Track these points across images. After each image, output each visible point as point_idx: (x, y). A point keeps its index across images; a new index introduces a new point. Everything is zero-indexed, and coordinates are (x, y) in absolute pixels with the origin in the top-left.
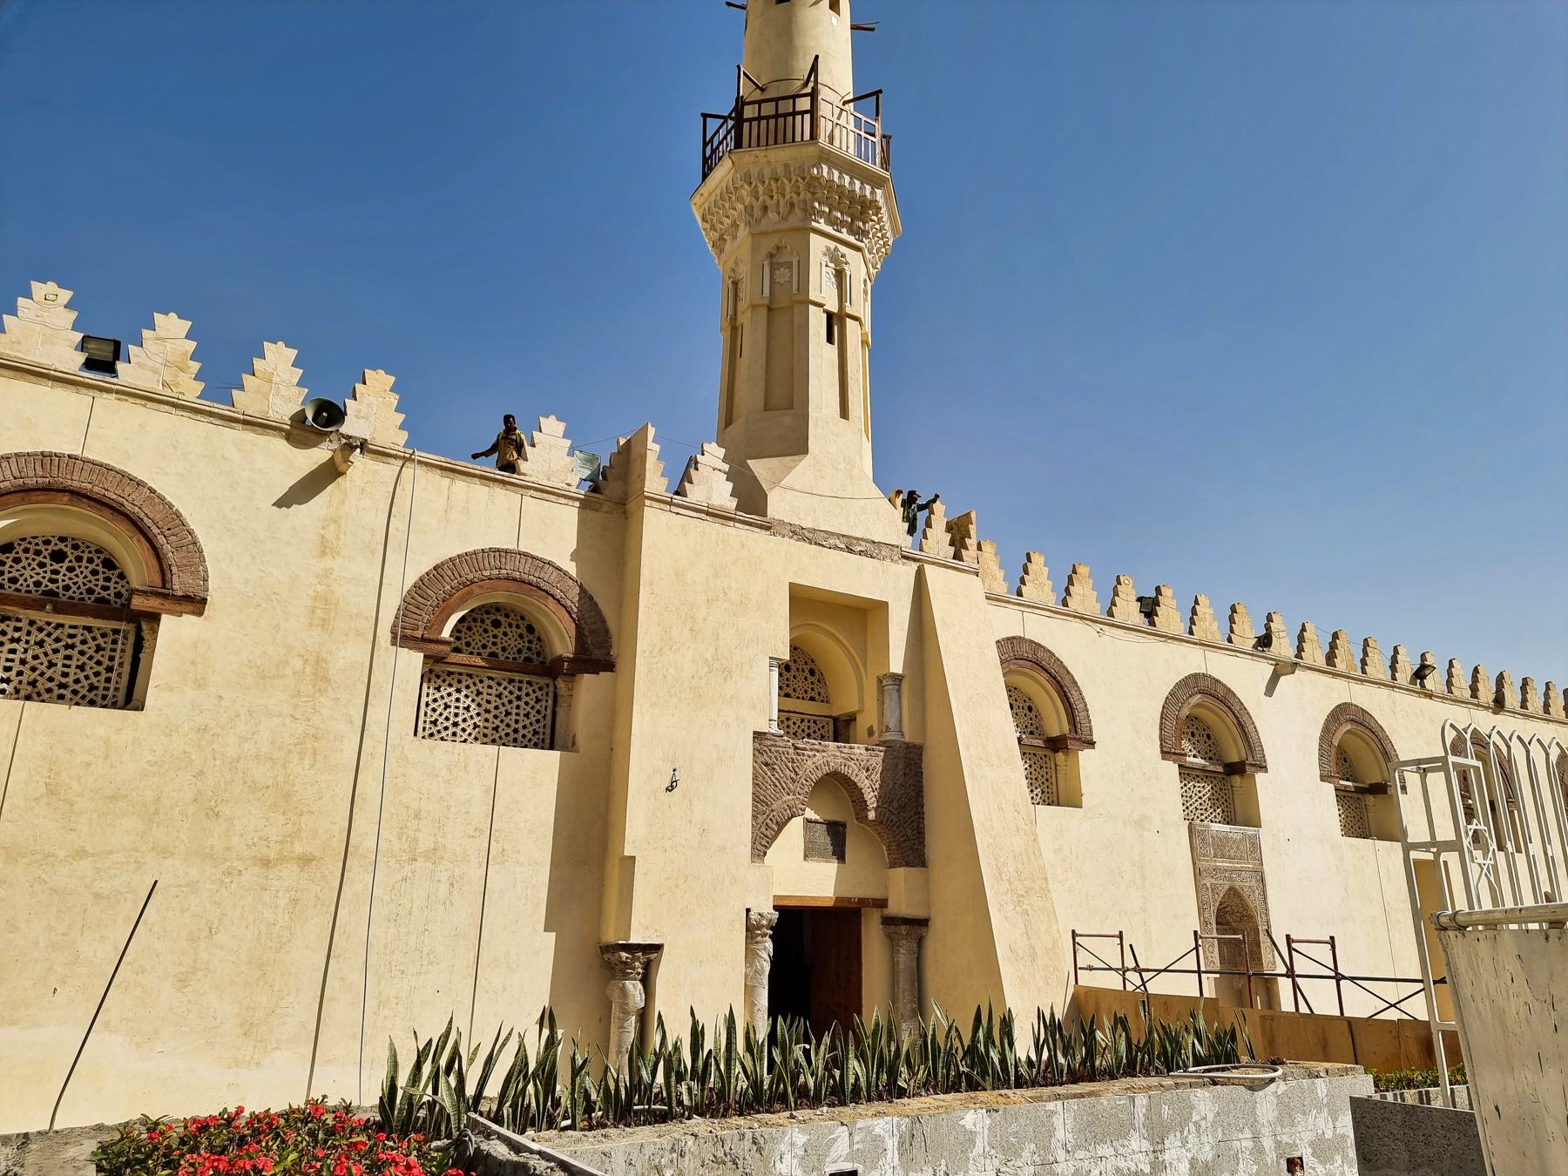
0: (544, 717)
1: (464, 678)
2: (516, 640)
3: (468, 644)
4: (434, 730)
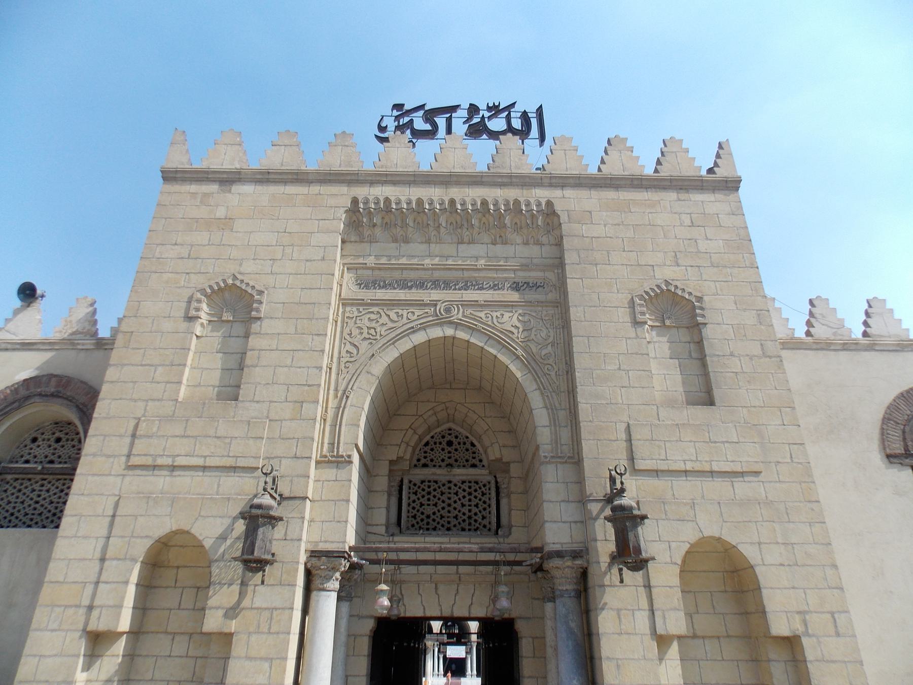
0: (489, 506)
2: (464, 453)
3: (432, 460)
4: (414, 522)
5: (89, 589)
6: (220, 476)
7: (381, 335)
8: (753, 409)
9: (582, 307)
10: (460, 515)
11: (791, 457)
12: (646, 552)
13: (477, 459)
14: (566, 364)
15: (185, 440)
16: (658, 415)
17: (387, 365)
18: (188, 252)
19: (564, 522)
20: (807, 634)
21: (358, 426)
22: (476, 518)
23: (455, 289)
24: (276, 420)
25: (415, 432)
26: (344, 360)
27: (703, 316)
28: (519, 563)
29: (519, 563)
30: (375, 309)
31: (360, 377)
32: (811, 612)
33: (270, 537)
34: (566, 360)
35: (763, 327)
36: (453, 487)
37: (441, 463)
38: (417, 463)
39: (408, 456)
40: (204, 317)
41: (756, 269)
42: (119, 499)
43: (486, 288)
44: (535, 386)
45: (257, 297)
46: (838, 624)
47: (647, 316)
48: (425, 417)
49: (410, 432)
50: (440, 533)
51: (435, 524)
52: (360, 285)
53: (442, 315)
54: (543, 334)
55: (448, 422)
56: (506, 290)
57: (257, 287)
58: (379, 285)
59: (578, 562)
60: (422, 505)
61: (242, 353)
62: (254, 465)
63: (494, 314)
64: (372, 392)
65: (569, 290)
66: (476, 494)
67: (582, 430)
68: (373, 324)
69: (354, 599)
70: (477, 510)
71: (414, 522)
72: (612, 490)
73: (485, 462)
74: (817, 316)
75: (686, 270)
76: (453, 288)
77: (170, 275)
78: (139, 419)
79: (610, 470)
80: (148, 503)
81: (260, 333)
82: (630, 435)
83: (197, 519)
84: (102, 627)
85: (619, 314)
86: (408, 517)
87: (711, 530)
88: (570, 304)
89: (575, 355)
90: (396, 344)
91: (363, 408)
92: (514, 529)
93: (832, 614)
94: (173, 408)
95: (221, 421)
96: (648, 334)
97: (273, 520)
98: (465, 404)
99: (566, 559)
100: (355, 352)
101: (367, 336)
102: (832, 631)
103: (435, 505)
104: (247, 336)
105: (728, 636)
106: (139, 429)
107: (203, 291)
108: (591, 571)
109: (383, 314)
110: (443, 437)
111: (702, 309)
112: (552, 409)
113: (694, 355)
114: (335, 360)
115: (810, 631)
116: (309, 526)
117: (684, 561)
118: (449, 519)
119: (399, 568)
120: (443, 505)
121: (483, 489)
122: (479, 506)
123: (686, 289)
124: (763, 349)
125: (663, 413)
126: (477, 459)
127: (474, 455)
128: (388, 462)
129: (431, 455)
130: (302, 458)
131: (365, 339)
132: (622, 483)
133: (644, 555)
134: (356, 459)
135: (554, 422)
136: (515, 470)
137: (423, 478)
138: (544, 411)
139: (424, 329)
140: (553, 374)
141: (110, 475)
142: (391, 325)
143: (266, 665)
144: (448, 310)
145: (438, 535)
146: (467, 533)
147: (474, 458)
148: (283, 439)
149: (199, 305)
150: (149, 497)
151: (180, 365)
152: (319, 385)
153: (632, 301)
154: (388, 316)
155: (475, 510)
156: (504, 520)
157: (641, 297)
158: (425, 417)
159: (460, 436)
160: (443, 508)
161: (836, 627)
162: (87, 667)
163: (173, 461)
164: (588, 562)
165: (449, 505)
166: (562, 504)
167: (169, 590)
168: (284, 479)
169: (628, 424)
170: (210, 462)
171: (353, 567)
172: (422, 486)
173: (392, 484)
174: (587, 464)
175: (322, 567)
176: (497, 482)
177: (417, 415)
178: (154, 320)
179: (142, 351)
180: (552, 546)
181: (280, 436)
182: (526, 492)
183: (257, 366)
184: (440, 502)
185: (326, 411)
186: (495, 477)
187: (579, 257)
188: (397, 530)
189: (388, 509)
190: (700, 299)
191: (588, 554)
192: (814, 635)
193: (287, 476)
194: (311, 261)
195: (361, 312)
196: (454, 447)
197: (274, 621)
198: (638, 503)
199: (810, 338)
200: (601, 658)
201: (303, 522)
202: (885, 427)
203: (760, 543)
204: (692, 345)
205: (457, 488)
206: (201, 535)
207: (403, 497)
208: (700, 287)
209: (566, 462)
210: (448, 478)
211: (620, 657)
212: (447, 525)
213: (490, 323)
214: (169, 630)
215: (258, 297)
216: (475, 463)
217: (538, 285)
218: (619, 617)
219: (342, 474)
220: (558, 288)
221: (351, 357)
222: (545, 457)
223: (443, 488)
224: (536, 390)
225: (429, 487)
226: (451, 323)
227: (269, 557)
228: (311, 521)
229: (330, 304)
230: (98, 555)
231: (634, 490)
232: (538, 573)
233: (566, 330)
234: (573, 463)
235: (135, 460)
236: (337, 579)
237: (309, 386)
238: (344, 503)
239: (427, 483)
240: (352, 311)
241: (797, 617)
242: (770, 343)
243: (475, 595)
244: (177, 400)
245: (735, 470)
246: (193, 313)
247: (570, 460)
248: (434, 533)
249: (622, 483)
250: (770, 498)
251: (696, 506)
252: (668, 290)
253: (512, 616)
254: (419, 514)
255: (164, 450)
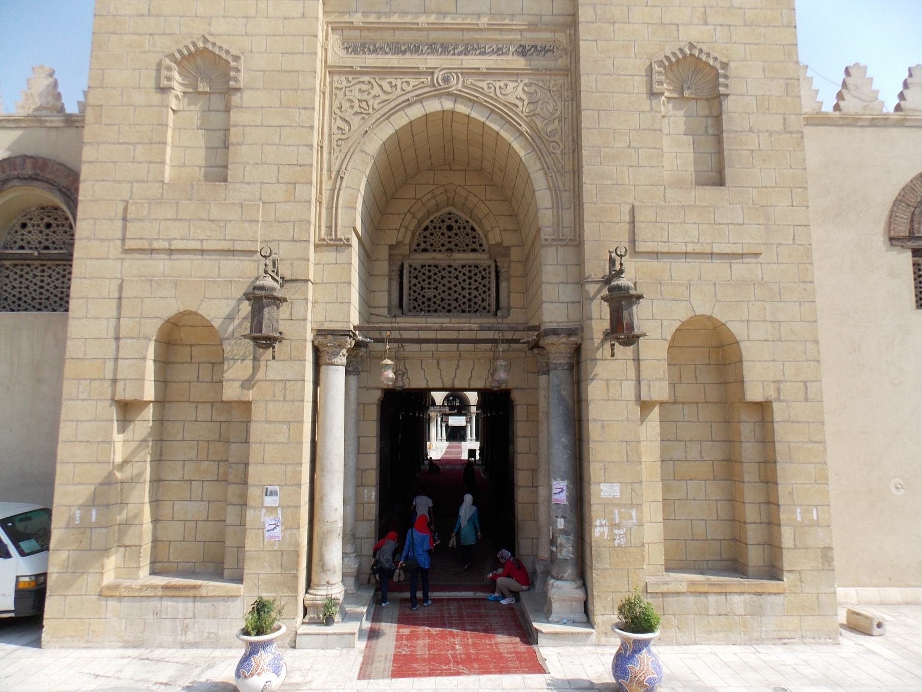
0: (489, 289)
1: (432, 268)
4: (416, 304)
5: (110, 365)
6: (220, 260)
7: (374, 109)
8: (763, 189)
9: (594, 76)
10: (460, 297)
11: (794, 239)
12: (639, 329)
13: (478, 243)
14: (573, 141)
15: (178, 224)
16: (665, 196)
17: (381, 142)
18: (147, 7)
19: (562, 303)
20: (778, 400)
21: (355, 208)
22: (476, 300)
23: (454, 54)
24: (269, 203)
25: (414, 216)
26: (335, 138)
27: (726, 86)
28: (517, 341)
29: (517, 341)
30: (366, 78)
31: (354, 156)
32: (786, 381)
33: (276, 317)
34: (573, 137)
35: (789, 99)
36: (453, 271)
37: (441, 248)
38: (417, 248)
39: (407, 241)
40: (178, 89)
41: (794, 29)
42: (122, 282)
43: (489, 53)
44: (539, 166)
45: (233, 64)
46: (808, 392)
47: (665, 86)
48: (424, 200)
49: (409, 216)
50: (441, 314)
51: (436, 306)
52: (347, 49)
53: (439, 85)
54: (550, 108)
55: (448, 206)
56: (511, 55)
57: (232, 52)
58: (369, 49)
59: (573, 339)
60: (422, 288)
61: (225, 130)
62: (253, 249)
63: (498, 84)
64: (367, 172)
65: (581, 55)
66: (476, 278)
67: (585, 212)
68: (365, 97)
69: (361, 373)
70: (477, 293)
71: (416, 304)
72: (610, 272)
73: (485, 247)
74: (850, 86)
75: (715, 30)
76: (452, 52)
77: (131, 36)
78: (127, 202)
79: (610, 252)
80: (151, 286)
81: (241, 107)
82: (634, 217)
83: (202, 301)
84: (129, 396)
85: (635, 83)
86: (410, 300)
87: (703, 309)
88: (581, 72)
89: (583, 131)
90: (390, 119)
91: (359, 190)
92: (512, 310)
93: (805, 383)
94: (161, 191)
95: (212, 204)
96: (664, 107)
97: (277, 301)
98: (466, 187)
99: (561, 336)
100: (346, 128)
101: (359, 110)
102: (802, 397)
103: (436, 288)
104: (228, 110)
105: (706, 402)
106: (129, 212)
107: (171, 57)
108: (584, 346)
109: (375, 84)
110: (443, 221)
111: (726, 77)
112: (555, 190)
113: (710, 131)
114: (326, 137)
115: (782, 398)
116: (313, 307)
117: (673, 338)
118: (450, 302)
119: (402, 346)
120: (444, 288)
121: (483, 273)
122: (479, 289)
123: (711, 53)
124: (785, 124)
125: (670, 194)
126: (478, 243)
127: (474, 240)
128: (387, 247)
129: (430, 240)
130: (301, 241)
131: (357, 113)
132: (621, 264)
133: (636, 331)
134: (355, 242)
135: (557, 204)
136: (515, 254)
137: (423, 262)
138: (548, 192)
139: (421, 101)
140: (558, 152)
141: (108, 258)
142: (384, 97)
143: (285, 427)
144: (446, 80)
145: (440, 317)
146: (467, 314)
147: (474, 243)
148: (279, 222)
149: (169, 73)
150: (151, 281)
151: (159, 143)
152: (311, 165)
153: (650, 68)
154: (381, 86)
155: (474, 293)
156: (503, 302)
157: (661, 63)
158: (424, 200)
159: (460, 221)
160: (444, 292)
161: (806, 393)
162: (122, 430)
163: (170, 245)
164: (582, 339)
165: (450, 289)
166: (561, 285)
167: (185, 365)
168: (284, 262)
169: (633, 206)
170: (207, 246)
171: (358, 344)
172: (423, 270)
173: (393, 268)
174: (587, 246)
175: (329, 344)
176: (497, 266)
177: (415, 199)
178: (123, 91)
179: (116, 127)
180: (548, 324)
181: (275, 219)
182: (525, 276)
183: (241, 144)
184: (440, 286)
185: (321, 193)
186: (495, 261)
187: (595, 13)
188: (399, 312)
189: (389, 292)
190: (725, 66)
191: (583, 331)
192: (784, 401)
193: (287, 259)
194: (289, 18)
195: (350, 82)
196: (454, 231)
197: (287, 391)
198: (635, 284)
199: (837, 113)
200: (588, 420)
201: (307, 303)
202: (895, 209)
203: (748, 321)
204: (710, 120)
205: (457, 273)
206: (208, 315)
207: (405, 281)
208: (727, 51)
209: (567, 245)
210: (448, 263)
211: (606, 419)
212: (447, 307)
213: (492, 95)
214: (192, 399)
215: (235, 63)
216: (476, 248)
217: (547, 49)
218: (608, 387)
219: (342, 257)
220: (569, 53)
221: (343, 134)
222: (546, 240)
223: (443, 273)
224: (540, 170)
225: (430, 271)
226: (449, 94)
227: (277, 335)
228: (315, 302)
229: (315, 72)
230: (112, 333)
231: (633, 271)
232: (534, 350)
233: (575, 102)
234: (576, 246)
235: (130, 244)
236: (344, 355)
237: (301, 166)
238: (346, 285)
239: (427, 268)
240: (341, 81)
241: (772, 386)
242: (793, 117)
243: (475, 369)
244: (163, 181)
245: (735, 251)
246: (164, 83)
247: (571, 243)
248: (434, 314)
249: (621, 264)
250: (766, 279)
251: (692, 287)
252: (691, 55)
253: (509, 387)
254: (420, 297)
255: (158, 233)
